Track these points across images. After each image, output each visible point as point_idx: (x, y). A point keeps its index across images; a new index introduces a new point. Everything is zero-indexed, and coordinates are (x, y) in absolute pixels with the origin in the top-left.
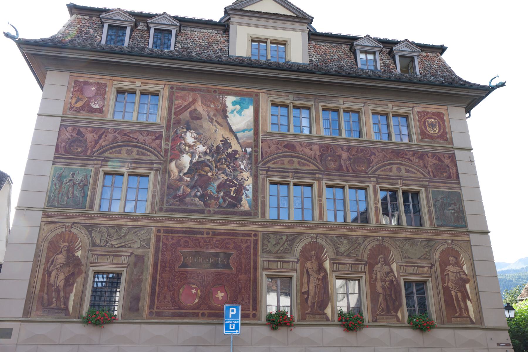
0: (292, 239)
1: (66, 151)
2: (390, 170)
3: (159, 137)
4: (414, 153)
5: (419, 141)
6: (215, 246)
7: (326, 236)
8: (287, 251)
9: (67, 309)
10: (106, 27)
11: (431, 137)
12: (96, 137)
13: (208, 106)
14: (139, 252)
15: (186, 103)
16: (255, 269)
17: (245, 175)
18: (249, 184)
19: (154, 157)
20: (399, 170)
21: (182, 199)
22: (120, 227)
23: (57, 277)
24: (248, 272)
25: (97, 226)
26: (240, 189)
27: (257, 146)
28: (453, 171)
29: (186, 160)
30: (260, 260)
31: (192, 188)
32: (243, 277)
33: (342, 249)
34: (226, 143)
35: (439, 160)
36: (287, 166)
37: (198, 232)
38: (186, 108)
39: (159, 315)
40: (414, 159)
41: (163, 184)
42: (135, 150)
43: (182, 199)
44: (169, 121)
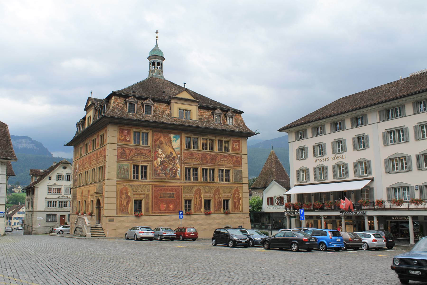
0: (192, 187)
1: (120, 157)
2: (222, 163)
3: (150, 151)
4: (230, 156)
5: (231, 151)
6: (170, 191)
7: (202, 186)
8: (191, 192)
9: (128, 212)
10: (128, 104)
11: (235, 150)
12: (129, 152)
13: (165, 139)
14: (147, 193)
15: (158, 138)
16: (181, 197)
17: (178, 165)
18: (179, 169)
19: (149, 159)
20: (225, 162)
21: (159, 175)
22: (141, 185)
23: (124, 202)
24: (179, 199)
25: (133, 185)
26: (176, 170)
27: (181, 154)
28: (240, 162)
29: (159, 160)
30: (183, 195)
31: (162, 170)
32: (178, 200)
33: (206, 191)
34: (171, 153)
35: (237, 158)
36: (191, 162)
37: (164, 186)
38: (158, 139)
39: (154, 213)
40: (230, 158)
41: (152, 169)
42: (142, 156)
43: (159, 175)
44: (153, 145)
